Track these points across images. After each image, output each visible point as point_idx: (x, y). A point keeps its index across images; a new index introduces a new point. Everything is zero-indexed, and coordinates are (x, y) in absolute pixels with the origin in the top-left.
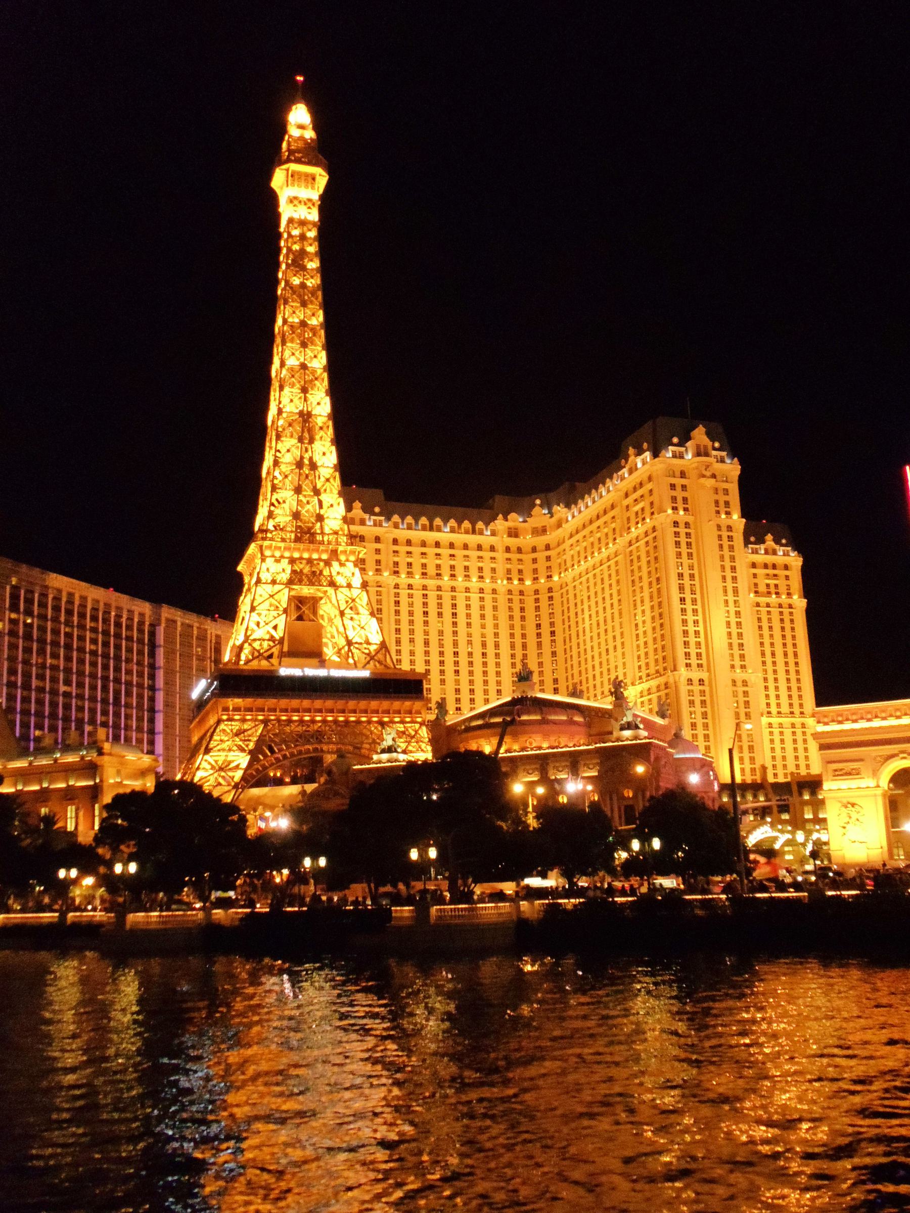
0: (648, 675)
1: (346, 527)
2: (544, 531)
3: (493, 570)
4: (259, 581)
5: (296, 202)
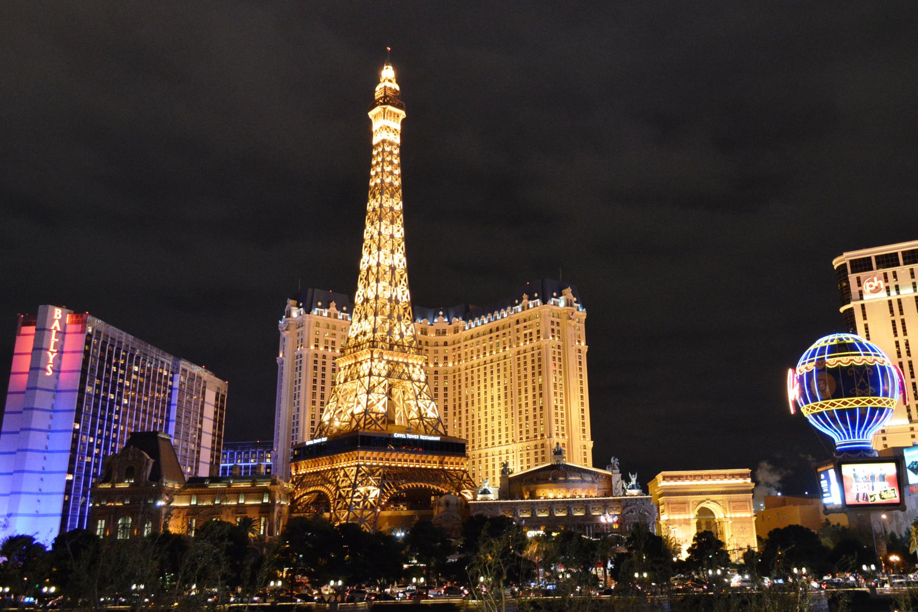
0: (527, 438)
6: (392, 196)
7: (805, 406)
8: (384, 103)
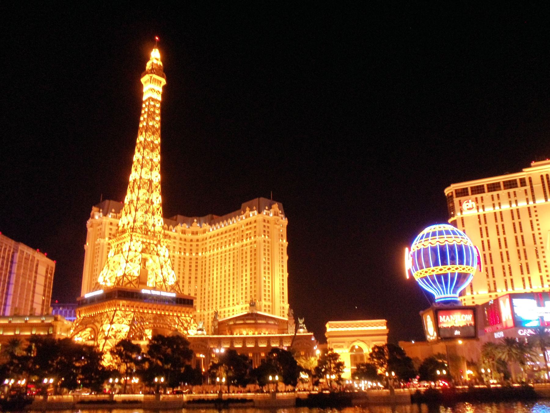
0: (246, 301)
1: (163, 231)
2: (197, 233)
3: (174, 247)
6: (153, 134)
7: (416, 273)
8: (152, 73)
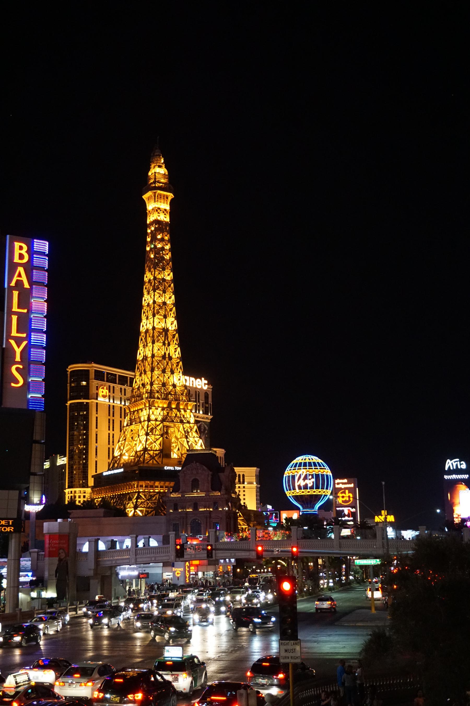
4: (149, 420)
5: (159, 211)
6: (164, 269)
